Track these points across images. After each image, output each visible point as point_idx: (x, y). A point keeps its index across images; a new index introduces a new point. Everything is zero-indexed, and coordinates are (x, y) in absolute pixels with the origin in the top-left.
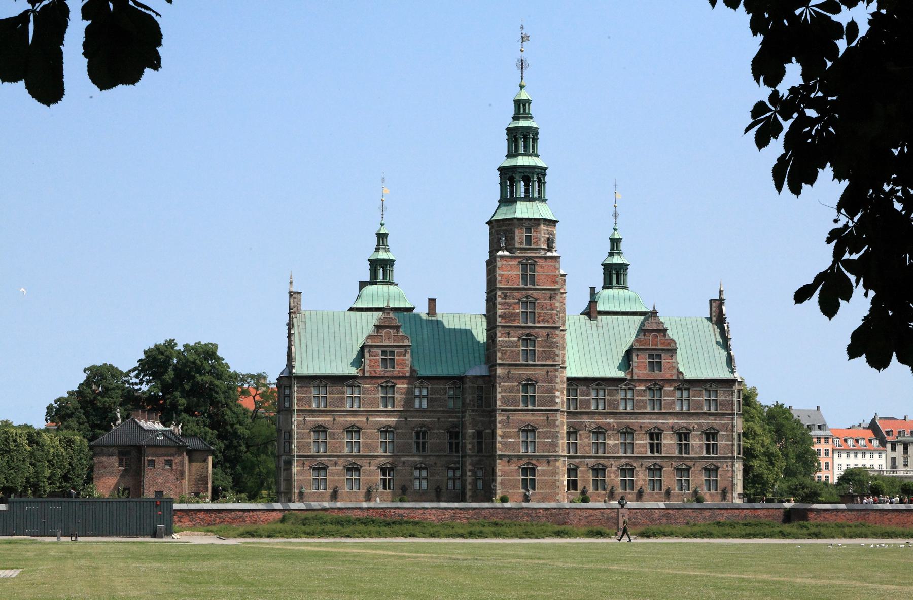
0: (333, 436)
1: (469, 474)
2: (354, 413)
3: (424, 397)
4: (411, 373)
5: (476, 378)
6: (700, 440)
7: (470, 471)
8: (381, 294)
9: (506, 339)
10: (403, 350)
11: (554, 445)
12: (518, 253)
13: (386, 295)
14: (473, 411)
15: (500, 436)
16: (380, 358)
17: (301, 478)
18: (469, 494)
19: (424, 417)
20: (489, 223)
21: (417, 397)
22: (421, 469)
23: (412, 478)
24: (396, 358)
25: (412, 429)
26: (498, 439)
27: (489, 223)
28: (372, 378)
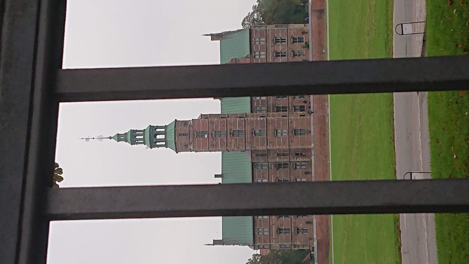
1: (298, 160)
7: (297, 159)
12: (191, 140)
14: (268, 158)
18: (307, 160)
20: (177, 153)
26: (281, 147)
27: (177, 153)
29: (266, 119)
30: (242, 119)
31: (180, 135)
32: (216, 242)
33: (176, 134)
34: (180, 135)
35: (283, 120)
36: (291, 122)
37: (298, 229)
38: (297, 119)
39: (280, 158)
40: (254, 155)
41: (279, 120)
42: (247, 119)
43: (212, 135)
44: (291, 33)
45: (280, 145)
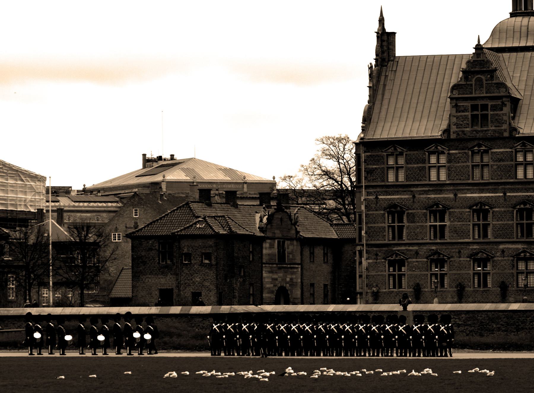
0: (412, 218)
2: (439, 187)
3: (530, 163)
4: (511, 132)
8: (517, 29)
10: (499, 102)
13: (524, 29)
16: (468, 114)
17: (373, 273)
19: (527, 190)
21: (521, 164)
22: (526, 260)
23: (514, 271)
24: (490, 113)
25: (514, 207)
28: (459, 140)
32: (386, 40)
37: (401, 263)
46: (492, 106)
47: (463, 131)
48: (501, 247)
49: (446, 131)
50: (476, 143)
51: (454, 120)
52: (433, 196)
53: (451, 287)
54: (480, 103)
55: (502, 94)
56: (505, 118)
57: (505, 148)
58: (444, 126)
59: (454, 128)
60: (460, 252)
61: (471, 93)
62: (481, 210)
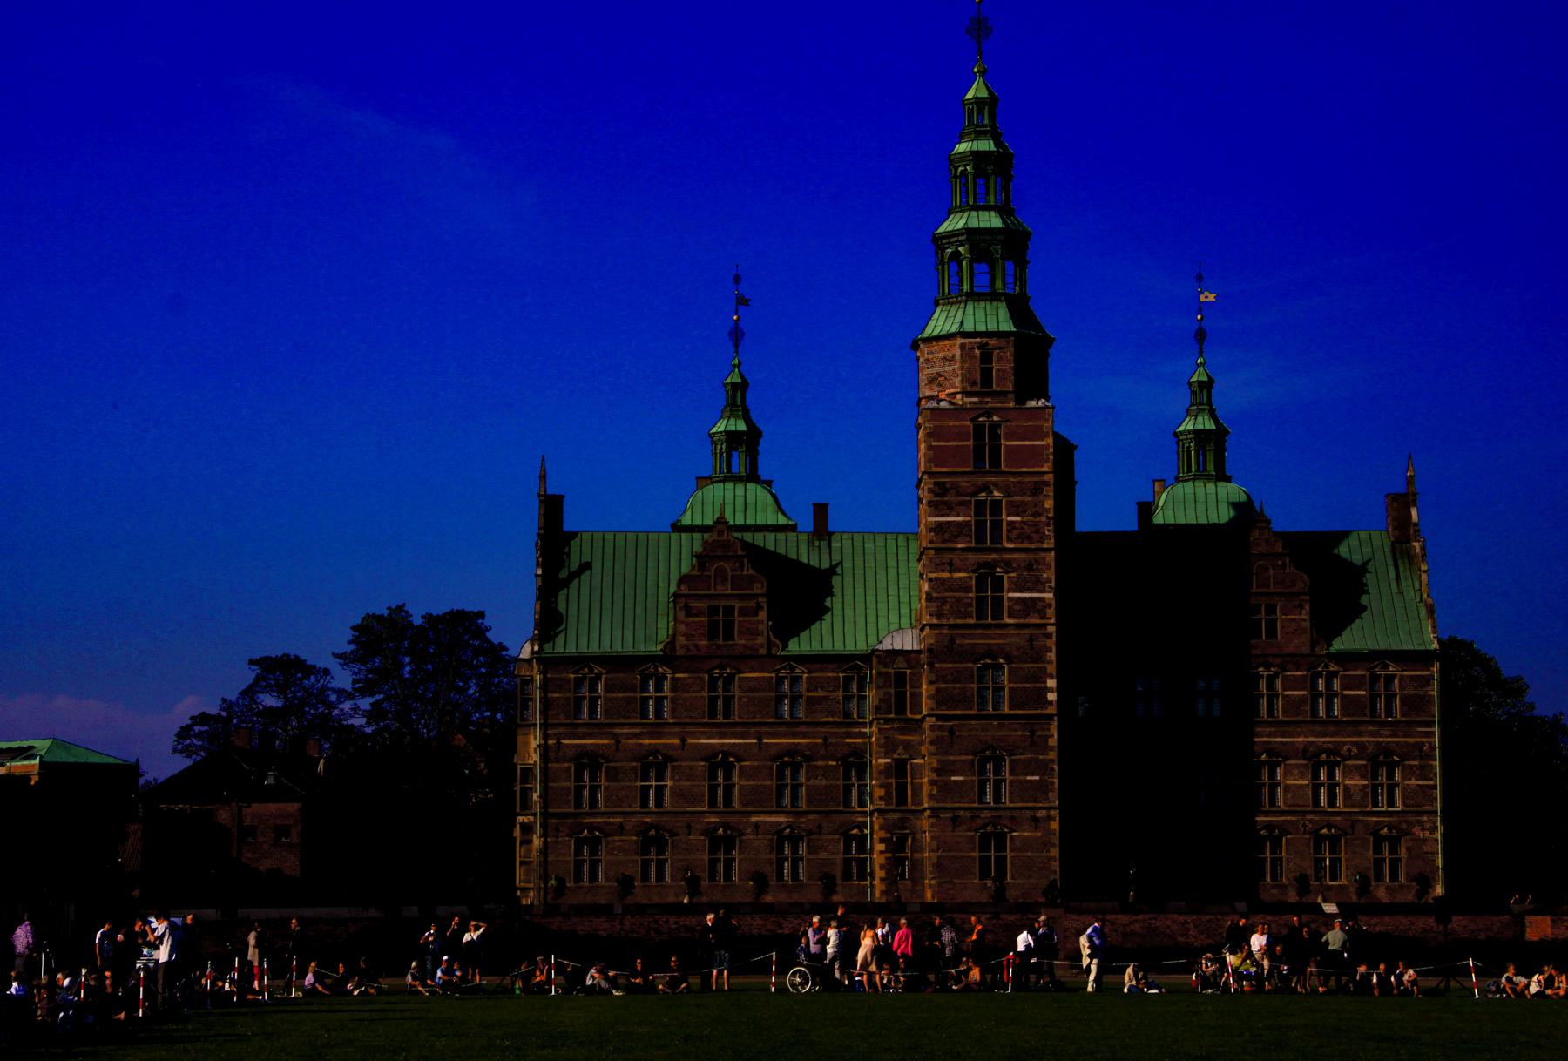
5: (894, 654)
6: (1363, 777)
7: (882, 840)
9: (946, 575)
10: (752, 604)
11: (1043, 787)
15: (934, 770)
19: (794, 736)
25: (774, 759)
29: (1050, 717)
30: (1051, 612)
31: (986, 357)
32: (552, 507)
33: (993, 342)
34: (986, 357)
35: (1043, 787)
36: (1036, 820)
38: (1047, 845)
39: (886, 771)
40: (900, 664)
41: (1043, 768)
42: (1049, 636)
43: (986, 488)
44: (1417, 831)
45: (938, 771)
46: (741, 609)
47: (696, 646)
48: (754, 819)
49: (671, 643)
50: (717, 661)
51: (682, 627)
52: (647, 742)
53: (607, 879)
54: (723, 603)
55: (756, 591)
56: (761, 627)
57: (762, 671)
58: (663, 635)
59: (681, 640)
60: (689, 827)
61: (709, 588)
62: (720, 762)
